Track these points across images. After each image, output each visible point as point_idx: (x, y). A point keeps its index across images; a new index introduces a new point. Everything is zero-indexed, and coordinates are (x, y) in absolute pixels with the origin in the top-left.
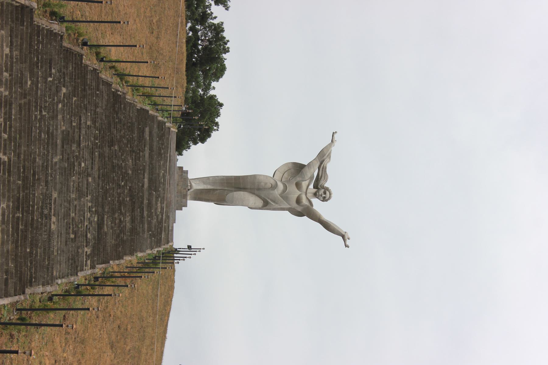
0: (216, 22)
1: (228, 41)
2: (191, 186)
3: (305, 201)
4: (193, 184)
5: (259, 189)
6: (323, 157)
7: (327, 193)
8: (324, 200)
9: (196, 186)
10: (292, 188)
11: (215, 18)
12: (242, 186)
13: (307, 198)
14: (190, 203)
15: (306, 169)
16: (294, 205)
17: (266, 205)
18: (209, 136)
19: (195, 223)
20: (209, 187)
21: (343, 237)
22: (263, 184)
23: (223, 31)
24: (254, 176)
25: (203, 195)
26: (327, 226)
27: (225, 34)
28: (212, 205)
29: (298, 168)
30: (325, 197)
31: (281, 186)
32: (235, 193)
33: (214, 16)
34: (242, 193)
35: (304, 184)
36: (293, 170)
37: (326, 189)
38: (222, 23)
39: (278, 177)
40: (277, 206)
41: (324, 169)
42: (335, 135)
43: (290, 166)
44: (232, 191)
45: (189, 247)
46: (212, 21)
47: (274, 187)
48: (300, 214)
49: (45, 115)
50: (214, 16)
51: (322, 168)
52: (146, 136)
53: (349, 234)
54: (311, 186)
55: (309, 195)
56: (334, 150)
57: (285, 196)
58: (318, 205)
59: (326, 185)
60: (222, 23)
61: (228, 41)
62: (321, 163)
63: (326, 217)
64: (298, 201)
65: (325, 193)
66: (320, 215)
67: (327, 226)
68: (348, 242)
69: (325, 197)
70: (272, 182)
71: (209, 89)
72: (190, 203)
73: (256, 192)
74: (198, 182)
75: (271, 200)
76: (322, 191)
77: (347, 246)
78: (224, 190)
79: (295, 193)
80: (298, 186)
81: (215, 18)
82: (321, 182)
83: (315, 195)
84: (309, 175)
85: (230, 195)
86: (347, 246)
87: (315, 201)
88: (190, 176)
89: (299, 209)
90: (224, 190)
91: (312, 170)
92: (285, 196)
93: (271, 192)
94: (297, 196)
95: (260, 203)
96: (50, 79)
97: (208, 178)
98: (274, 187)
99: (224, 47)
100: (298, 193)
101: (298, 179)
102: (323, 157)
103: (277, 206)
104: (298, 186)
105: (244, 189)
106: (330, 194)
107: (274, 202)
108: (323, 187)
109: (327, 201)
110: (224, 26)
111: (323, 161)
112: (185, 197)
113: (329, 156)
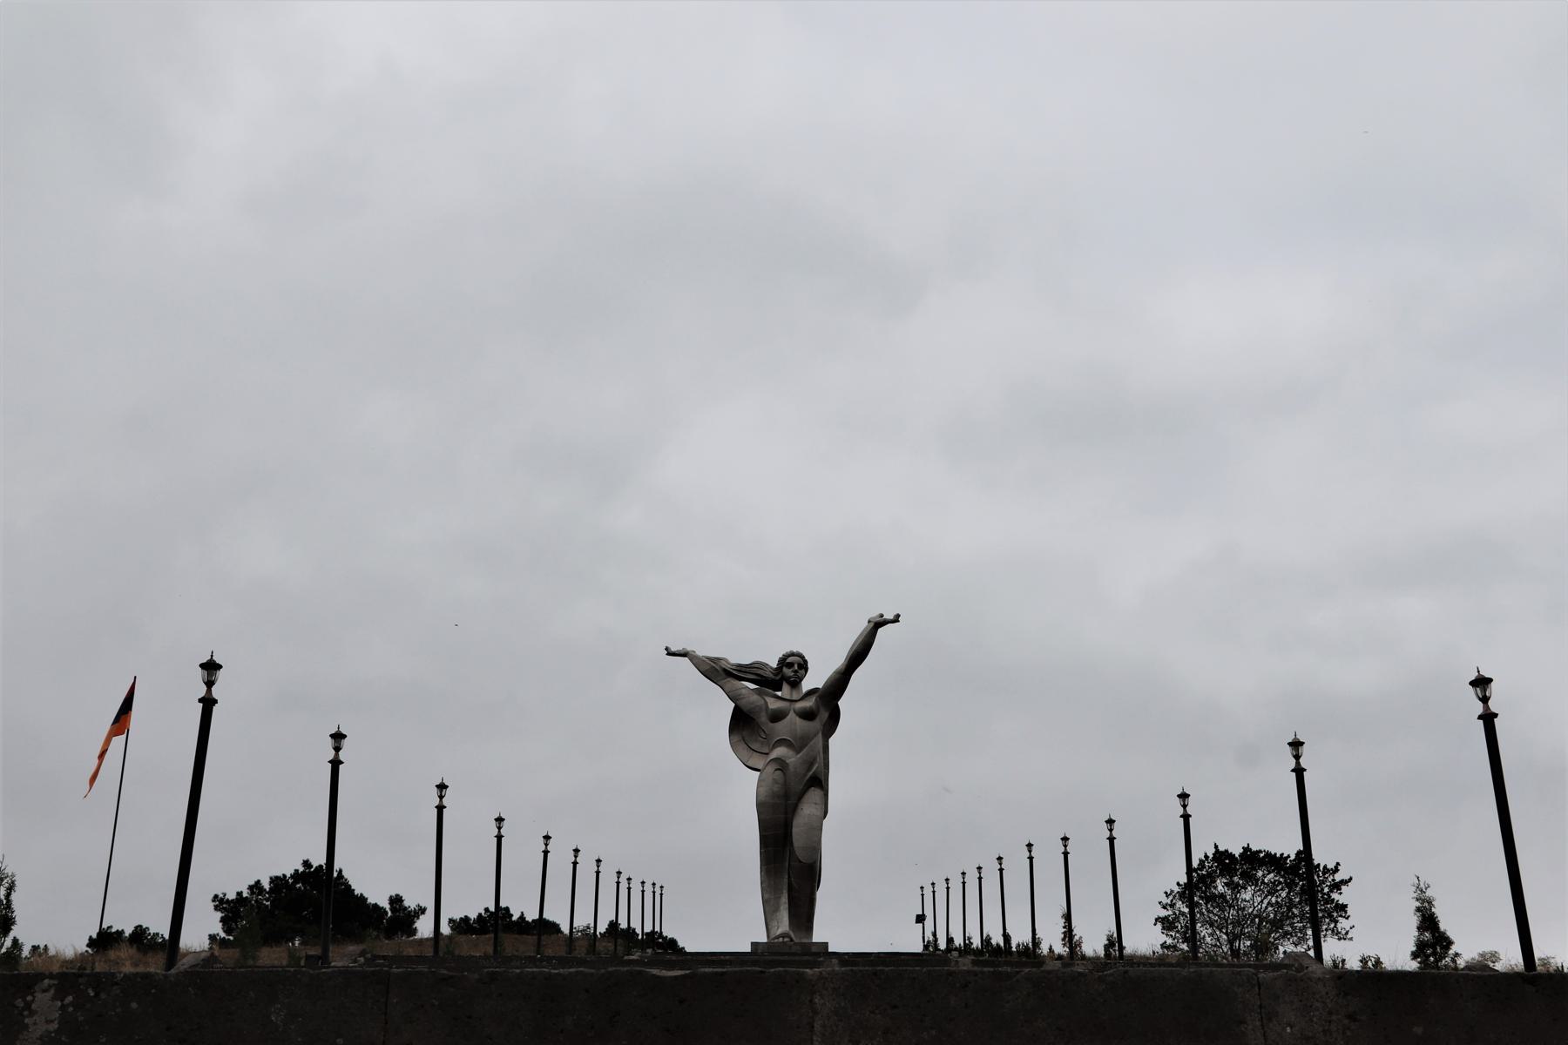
2: (783, 935)
3: (809, 703)
4: (779, 932)
6: (716, 671)
7: (790, 660)
8: (804, 666)
9: (783, 925)
10: (782, 729)
14: (818, 936)
15: (742, 703)
16: (816, 725)
17: (819, 781)
18: (673, 942)
20: (784, 899)
21: (878, 624)
23: (466, 919)
24: (760, 805)
25: (803, 913)
26: (858, 656)
27: (473, 916)
28: (819, 894)
29: (743, 723)
31: (780, 752)
32: (796, 844)
34: (795, 830)
35: (773, 704)
37: (783, 662)
38: (451, 921)
40: (820, 759)
42: (673, 649)
43: (736, 738)
44: (792, 852)
45: (920, 919)
47: (781, 764)
53: (873, 614)
55: (795, 697)
56: (702, 652)
57: (798, 744)
58: (815, 679)
59: (774, 665)
63: (838, 660)
64: (808, 715)
65: (790, 665)
67: (858, 656)
68: (890, 617)
70: (770, 769)
72: (818, 936)
75: (809, 769)
76: (788, 672)
77: (896, 619)
78: (790, 867)
79: (792, 724)
80: (777, 717)
82: (768, 674)
83: (795, 684)
84: (755, 697)
85: (800, 854)
86: (896, 619)
87: (807, 684)
90: (790, 867)
92: (798, 744)
93: (791, 768)
95: (814, 794)
97: (765, 902)
98: (781, 764)
100: (792, 715)
101: (763, 719)
102: (716, 671)
103: (820, 759)
104: (777, 717)
105: (787, 826)
106: (792, 654)
107: (811, 764)
108: (779, 669)
110: (457, 917)
113: (716, 660)
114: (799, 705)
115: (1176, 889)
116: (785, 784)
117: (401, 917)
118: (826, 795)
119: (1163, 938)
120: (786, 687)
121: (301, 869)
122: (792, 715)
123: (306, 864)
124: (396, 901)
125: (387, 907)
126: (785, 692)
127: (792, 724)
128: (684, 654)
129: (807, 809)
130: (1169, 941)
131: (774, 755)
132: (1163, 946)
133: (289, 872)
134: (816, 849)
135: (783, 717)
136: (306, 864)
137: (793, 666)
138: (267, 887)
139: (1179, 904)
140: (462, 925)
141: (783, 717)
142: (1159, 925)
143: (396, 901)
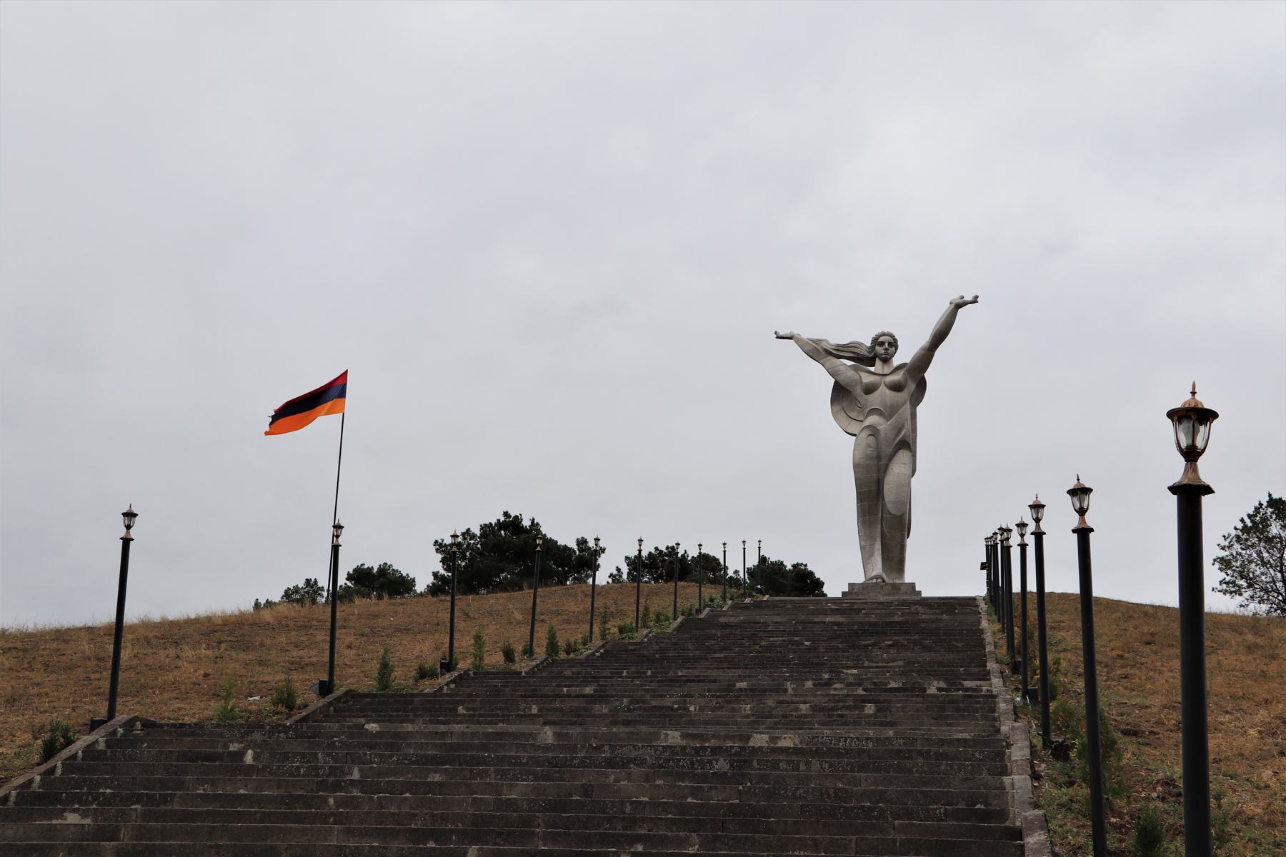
0: (625, 570)
1: (656, 549)
2: (877, 577)
4: (874, 574)
5: (879, 458)
6: (819, 352)
8: (894, 344)
9: (877, 568)
10: (875, 400)
11: (618, 570)
12: (874, 488)
13: (891, 373)
14: (908, 578)
16: (905, 395)
17: (907, 444)
18: (811, 574)
19: (944, 567)
20: (878, 546)
21: (959, 306)
22: (869, 451)
24: (856, 466)
25: (894, 557)
26: (940, 336)
28: (911, 543)
29: (841, 393)
30: (890, 344)
31: (873, 419)
33: (615, 572)
34: (886, 487)
35: (867, 379)
36: (844, 404)
37: (876, 342)
38: (627, 558)
39: (856, 428)
40: (908, 425)
41: (840, 348)
42: (781, 333)
43: (837, 408)
44: (884, 505)
46: (625, 576)
47: (873, 431)
48: (922, 386)
49: (361, 771)
50: (615, 572)
51: (838, 352)
52: (737, 620)
53: (955, 297)
54: (872, 369)
55: (887, 371)
56: (807, 334)
57: (889, 412)
58: (903, 356)
59: (868, 344)
60: (627, 558)
61: (656, 549)
62: (829, 353)
64: (897, 387)
65: (882, 344)
66: (922, 349)
67: (940, 336)
68: (968, 298)
69: (890, 344)
70: (864, 435)
71: (738, 580)
72: (908, 578)
73: (884, 462)
74: (870, 566)
75: (897, 435)
76: (880, 350)
77: (975, 301)
78: (884, 518)
79: (883, 395)
80: (870, 389)
81: (618, 570)
82: (864, 352)
83: (886, 360)
84: (851, 373)
85: (890, 507)
86: (975, 301)
87: (897, 360)
88: (860, 579)
89: (912, 386)
90: (884, 518)
91: (842, 368)
92: (889, 412)
93: (882, 435)
94: (888, 391)
95: (903, 456)
96: (249, 758)
97: (862, 548)
98: (873, 431)
99: (666, 555)
100: (883, 389)
102: (819, 352)
103: (908, 425)
104: (870, 389)
105: (879, 483)
106: (884, 335)
107: (900, 430)
108: (872, 348)
109: (896, 341)
111: (825, 350)
112: (896, 588)
113: (817, 342)
114: (889, 379)
115: (1234, 533)
116: (878, 447)
117: (586, 558)
118: (914, 456)
119: (1222, 575)
120: (878, 362)
121: (502, 519)
122: (883, 389)
123: (506, 514)
124: (582, 542)
125: (575, 548)
126: (878, 367)
127: (883, 395)
128: (790, 338)
129: (898, 468)
130: (1228, 578)
131: (867, 423)
132: (1221, 583)
133: (494, 522)
134: (906, 503)
135: (878, 388)
136: (506, 514)
137: (884, 347)
138: (478, 533)
139: (1237, 547)
140: (636, 564)
141: (878, 388)
142: (1217, 565)
143: (582, 542)
